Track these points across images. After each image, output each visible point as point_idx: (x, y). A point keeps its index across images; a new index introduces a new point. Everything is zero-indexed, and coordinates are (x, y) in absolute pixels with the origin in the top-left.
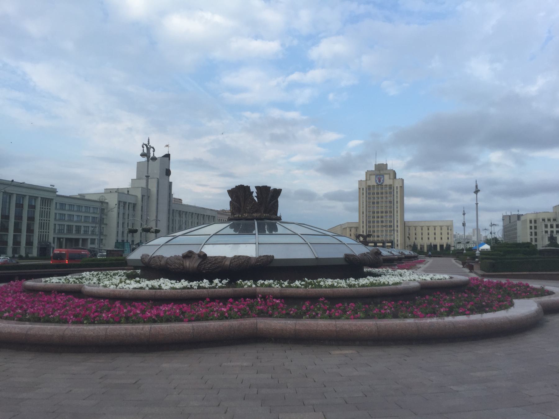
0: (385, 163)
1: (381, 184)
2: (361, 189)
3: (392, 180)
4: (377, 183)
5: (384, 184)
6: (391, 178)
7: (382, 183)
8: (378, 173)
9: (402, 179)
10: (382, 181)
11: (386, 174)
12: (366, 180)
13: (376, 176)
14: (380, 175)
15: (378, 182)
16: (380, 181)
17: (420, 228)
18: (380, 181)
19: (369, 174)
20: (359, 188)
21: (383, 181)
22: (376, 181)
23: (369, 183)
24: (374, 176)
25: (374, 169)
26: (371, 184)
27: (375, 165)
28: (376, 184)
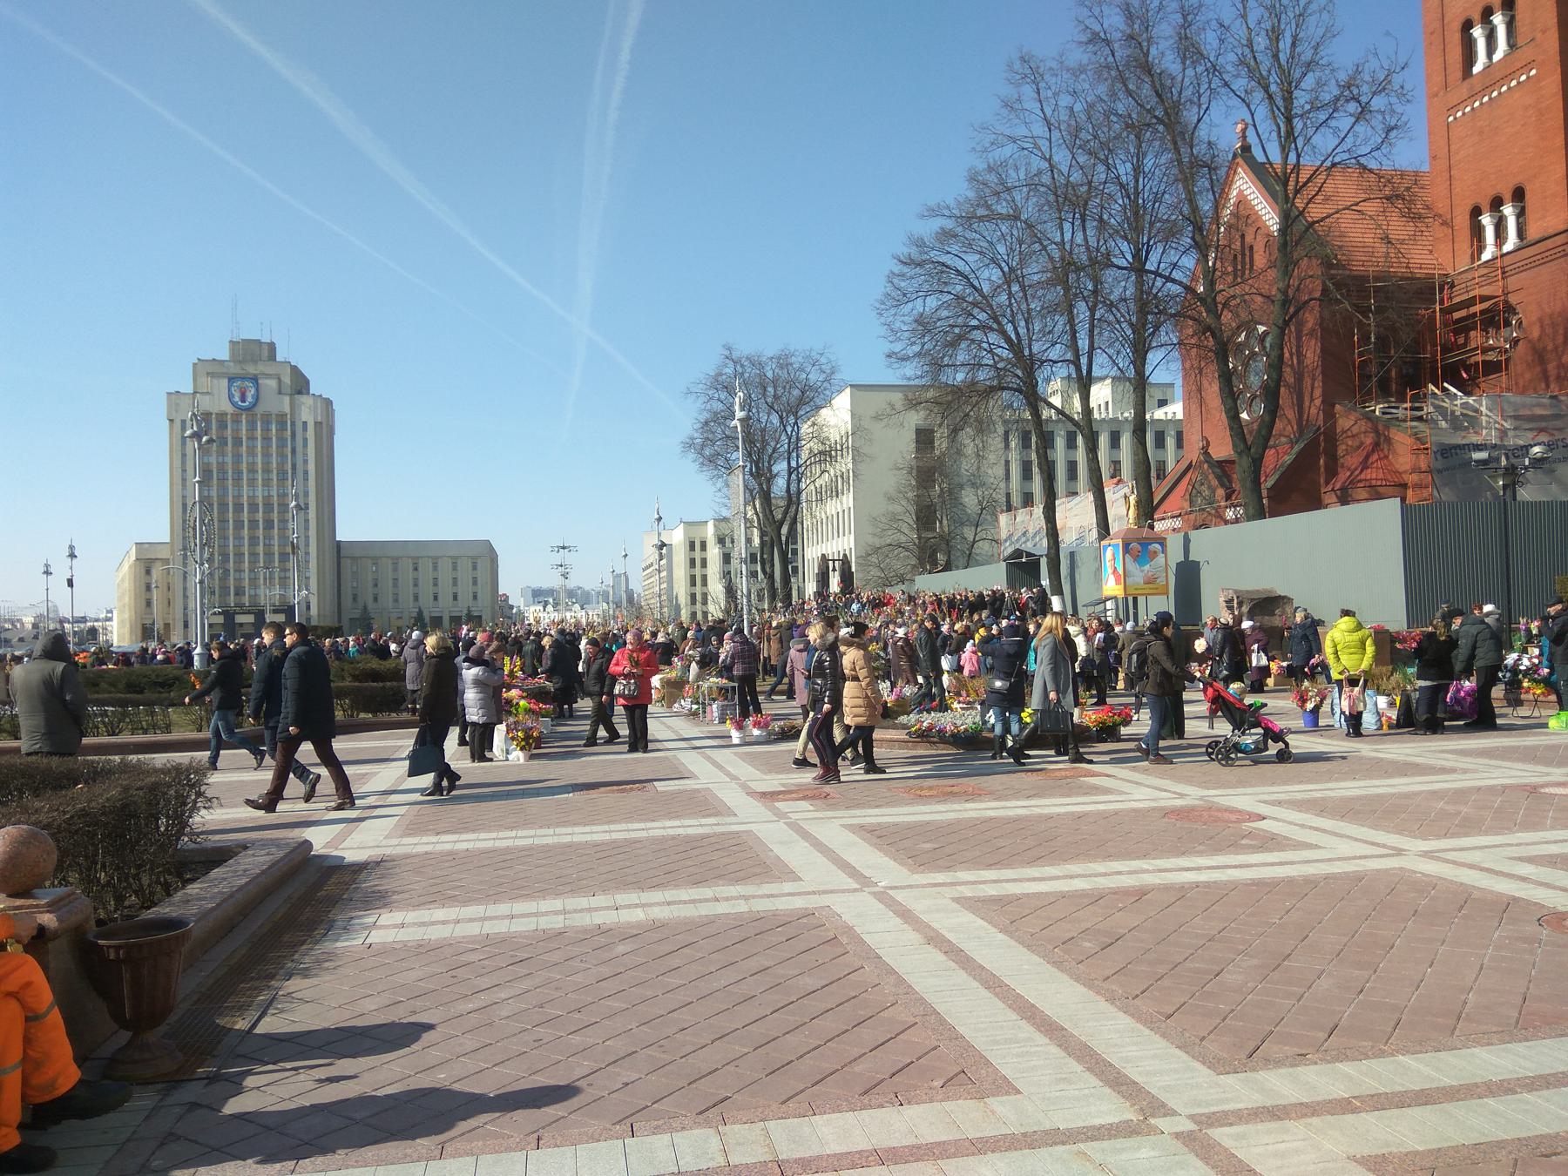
0: (265, 339)
1: (248, 409)
2: (178, 425)
3: (287, 399)
4: (234, 404)
5: (260, 410)
6: (283, 391)
7: (254, 405)
8: (235, 369)
9: (321, 396)
10: (249, 399)
11: (268, 376)
12: (195, 393)
13: (231, 380)
14: (243, 378)
15: (237, 399)
16: (243, 400)
17: (390, 562)
18: (243, 400)
19: (206, 369)
20: (171, 421)
21: (257, 398)
22: (231, 397)
23: (207, 404)
24: (225, 382)
25: (224, 354)
26: (215, 410)
27: (231, 341)
28: (229, 409)
